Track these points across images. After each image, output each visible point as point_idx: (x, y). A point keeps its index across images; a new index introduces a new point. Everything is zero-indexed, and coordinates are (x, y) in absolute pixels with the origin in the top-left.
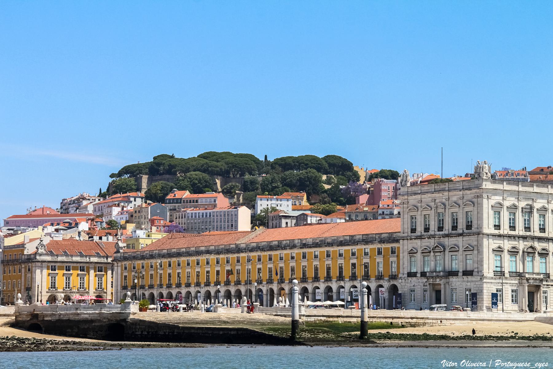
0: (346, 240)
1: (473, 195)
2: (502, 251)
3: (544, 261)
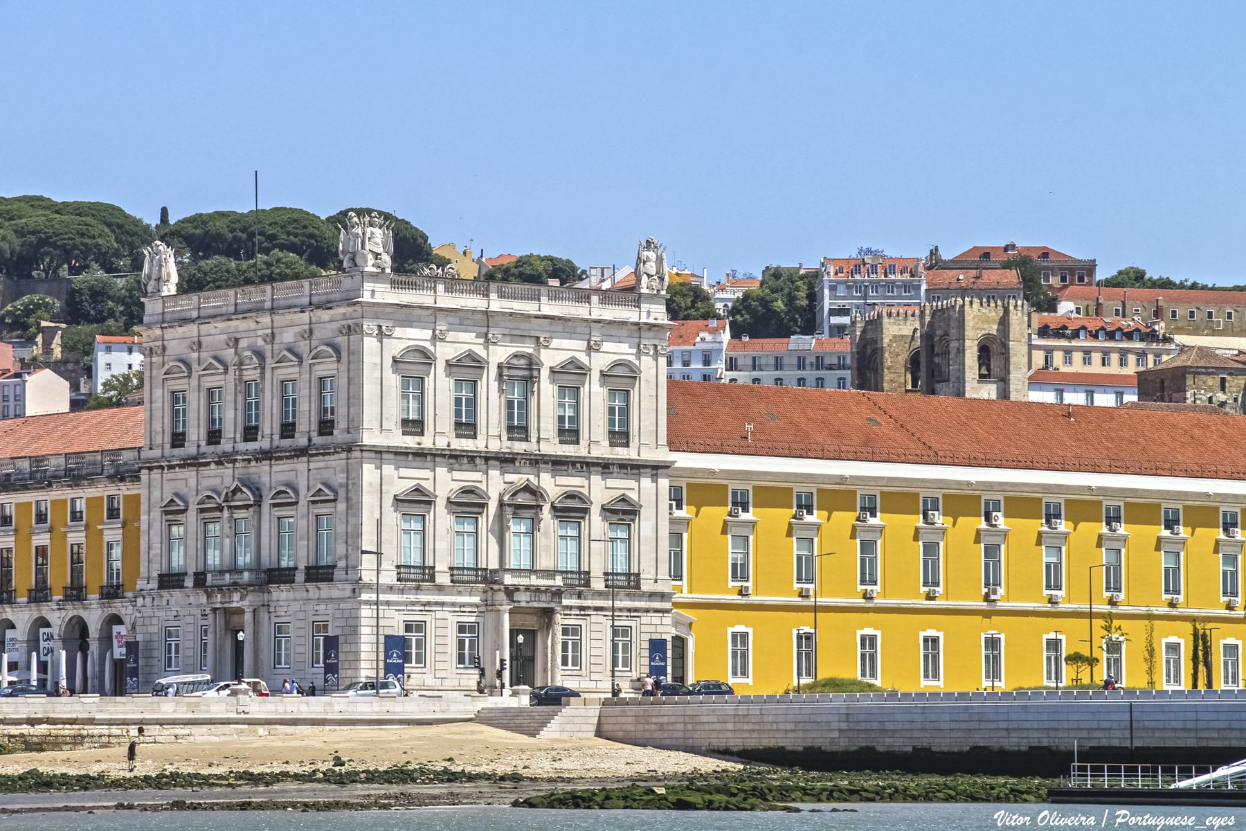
0: (20, 472)
1: (335, 325)
2: (429, 503)
3: (572, 532)
